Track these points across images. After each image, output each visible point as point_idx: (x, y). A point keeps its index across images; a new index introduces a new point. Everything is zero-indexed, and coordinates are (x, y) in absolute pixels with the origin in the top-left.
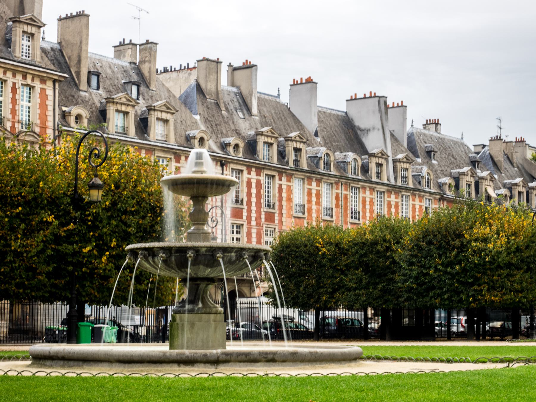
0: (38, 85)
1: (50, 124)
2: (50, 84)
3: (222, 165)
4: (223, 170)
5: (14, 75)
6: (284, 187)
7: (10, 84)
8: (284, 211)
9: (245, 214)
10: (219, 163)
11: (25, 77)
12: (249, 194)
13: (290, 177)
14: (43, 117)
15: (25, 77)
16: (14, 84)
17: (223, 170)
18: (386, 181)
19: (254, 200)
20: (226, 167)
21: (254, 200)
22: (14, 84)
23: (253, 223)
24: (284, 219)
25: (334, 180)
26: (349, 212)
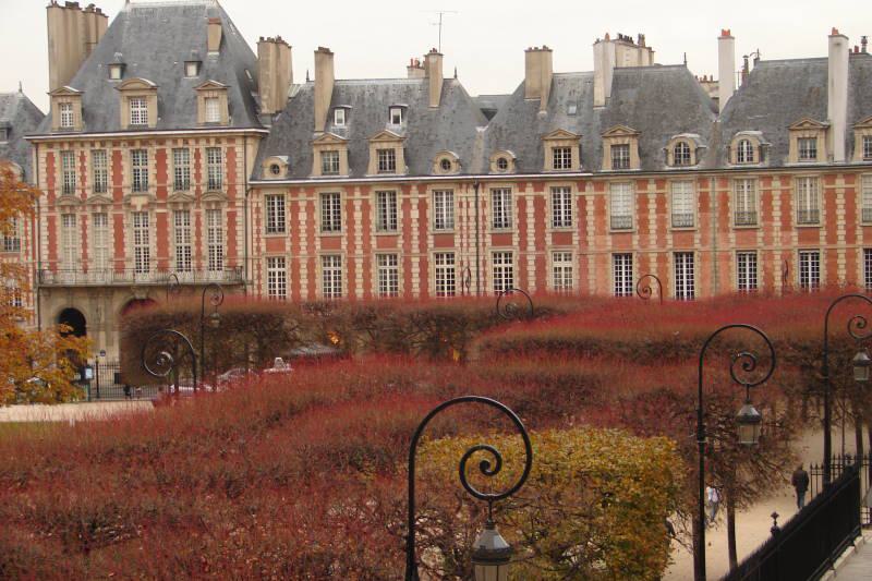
0: (224, 146)
1: (240, 179)
2: (239, 142)
3: (476, 187)
4: (477, 192)
5: (197, 141)
6: (590, 200)
7: (192, 151)
8: (591, 228)
9: (516, 239)
10: (471, 186)
11: (208, 141)
12: (523, 215)
13: (599, 185)
14: (232, 175)
15: (208, 141)
16: (197, 150)
17: (477, 192)
18: (824, 163)
19: (531, 221)
20: (483, 187)
21: (531, 221)
22: (197, 150)
23: (531, 247)
24: (591, 238)
25: (692, 177)
26: (731, 215)
